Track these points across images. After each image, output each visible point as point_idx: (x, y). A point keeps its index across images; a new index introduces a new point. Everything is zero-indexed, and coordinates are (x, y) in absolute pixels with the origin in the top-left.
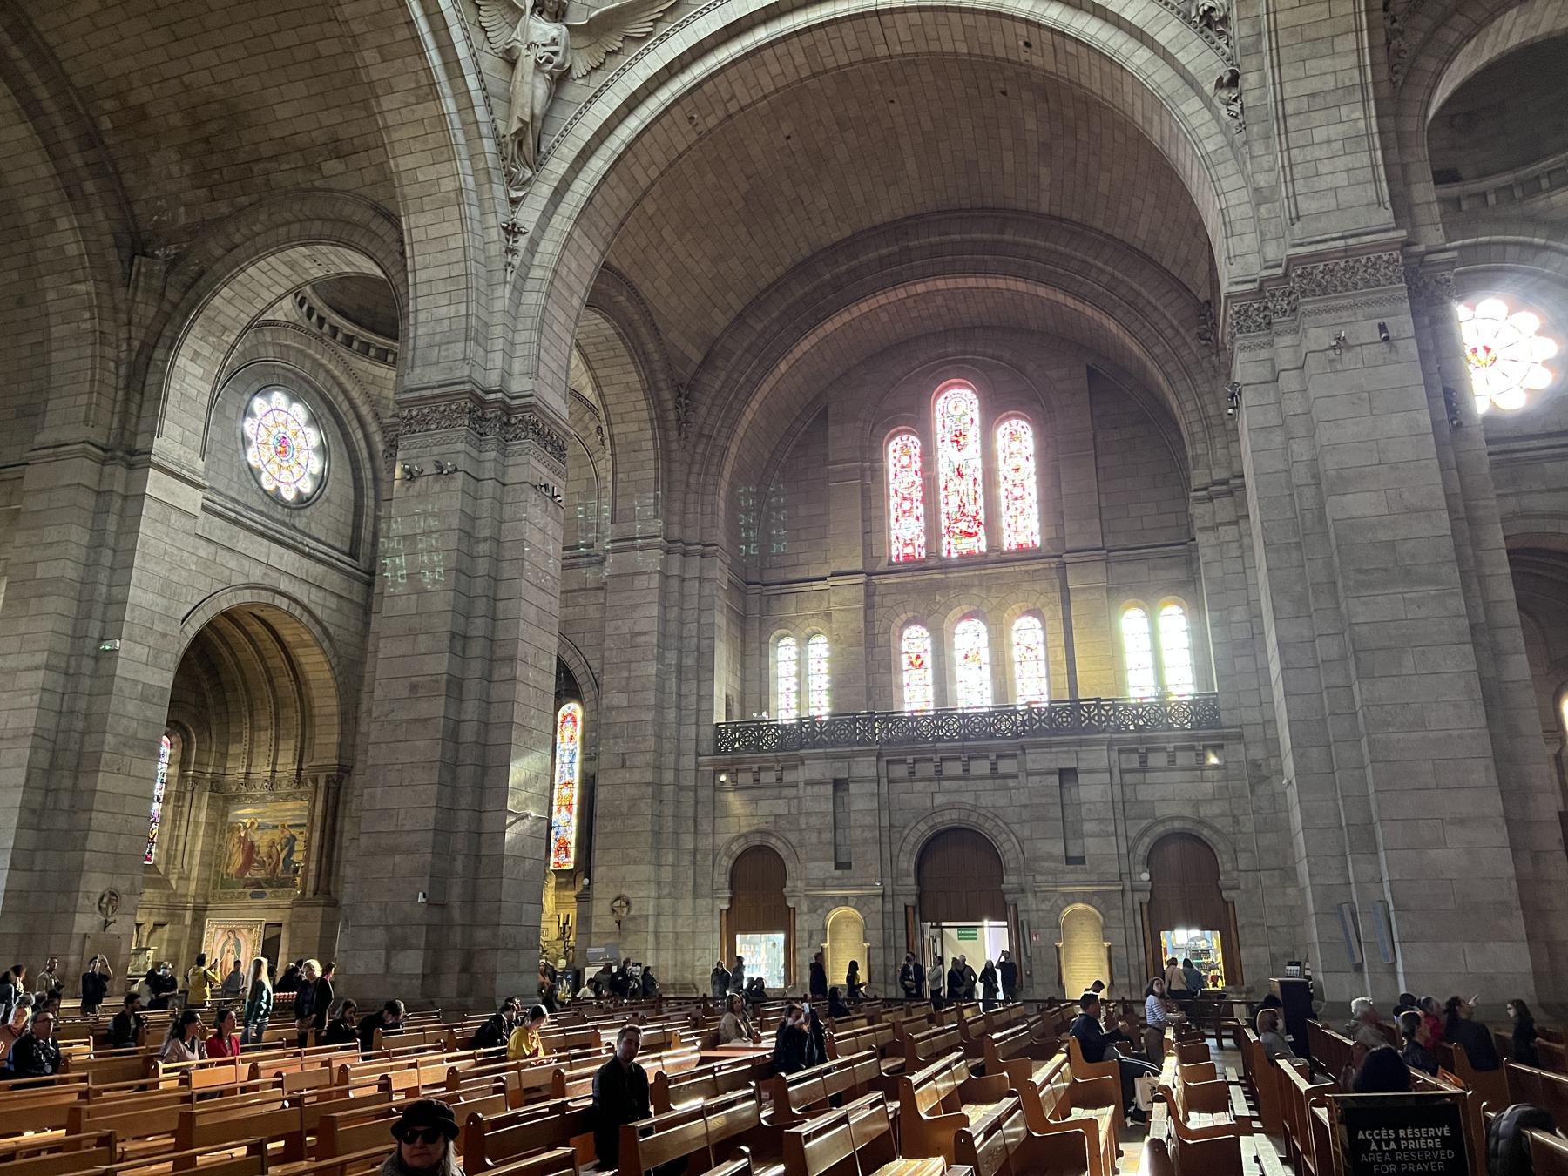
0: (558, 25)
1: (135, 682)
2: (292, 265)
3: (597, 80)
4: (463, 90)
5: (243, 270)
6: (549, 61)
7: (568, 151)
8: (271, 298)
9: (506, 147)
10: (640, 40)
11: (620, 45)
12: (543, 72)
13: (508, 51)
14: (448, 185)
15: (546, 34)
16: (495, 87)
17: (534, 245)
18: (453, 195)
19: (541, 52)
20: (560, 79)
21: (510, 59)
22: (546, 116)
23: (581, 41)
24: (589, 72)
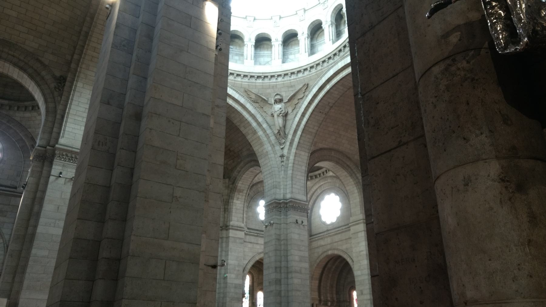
0: (281, 104)
1: (232, 284)
2: (252, 172)
3: (295, 112)
5: (242, 176)
6: (280, 113)
7: (292, 132)
8: (251, 180)
11: (298, 102)
13: (272, 114)
14: (265, 151)
15: (278, 108)
16: (271, 123)
17: (288, 158)
19: (278, 112)
21: (272, 115)
22: (284, 126)
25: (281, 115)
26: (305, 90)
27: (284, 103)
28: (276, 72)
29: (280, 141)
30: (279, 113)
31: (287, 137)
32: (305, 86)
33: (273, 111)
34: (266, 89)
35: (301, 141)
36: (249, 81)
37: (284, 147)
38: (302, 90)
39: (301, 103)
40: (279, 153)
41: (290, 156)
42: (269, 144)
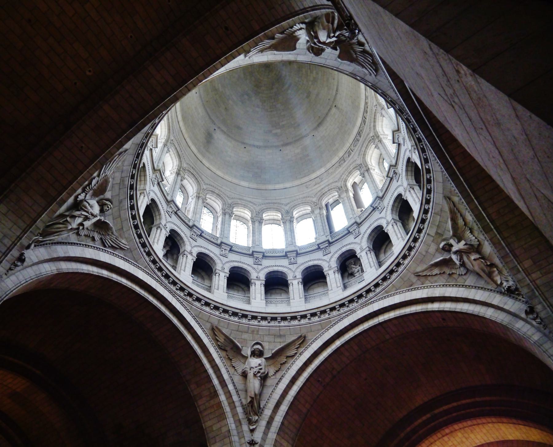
0: (261, 359)
3: (279, 375)
4: (227, 391)
6: (259, 372)
9: (247, 409)
10: (292, 356)
11: (286, 360)
12: (257, 377)
14: (224, 430)
15: (256, 363)
18: (226, 433)
19: (256, 370)
20: (264, 378)
21: (244, 375)
22: (261, 394)
23: (271, 362)
24: (275, 373)
25: (259, 374)
26: (300, 344)
27: (265, 359)
28: (260, 313)
29: (250, 417)
30: (258, 370)
31: (261, 413)
32: (301, 338)
33: (247, 367)
34: (242, 332)
35: (286, 422)
36: (220, 315)
37: (256, 428)
38: (295, 344)
39: (291, 363)
40: (248, 437)
41: (265, 444)
42: (232, 419)
